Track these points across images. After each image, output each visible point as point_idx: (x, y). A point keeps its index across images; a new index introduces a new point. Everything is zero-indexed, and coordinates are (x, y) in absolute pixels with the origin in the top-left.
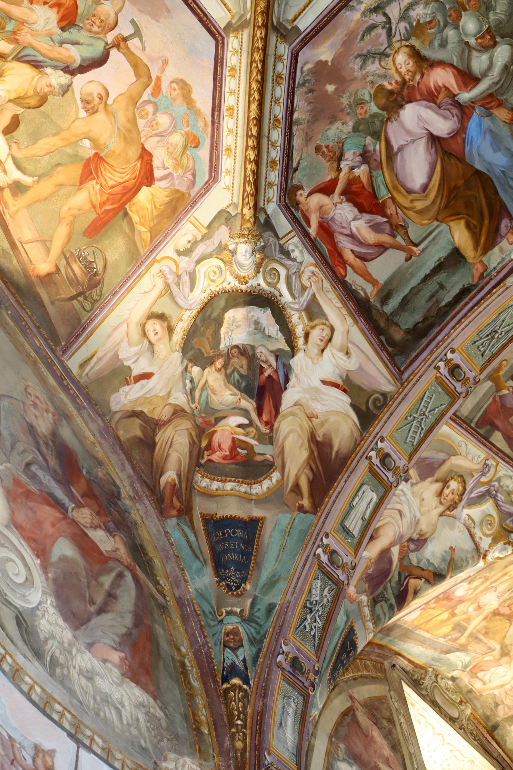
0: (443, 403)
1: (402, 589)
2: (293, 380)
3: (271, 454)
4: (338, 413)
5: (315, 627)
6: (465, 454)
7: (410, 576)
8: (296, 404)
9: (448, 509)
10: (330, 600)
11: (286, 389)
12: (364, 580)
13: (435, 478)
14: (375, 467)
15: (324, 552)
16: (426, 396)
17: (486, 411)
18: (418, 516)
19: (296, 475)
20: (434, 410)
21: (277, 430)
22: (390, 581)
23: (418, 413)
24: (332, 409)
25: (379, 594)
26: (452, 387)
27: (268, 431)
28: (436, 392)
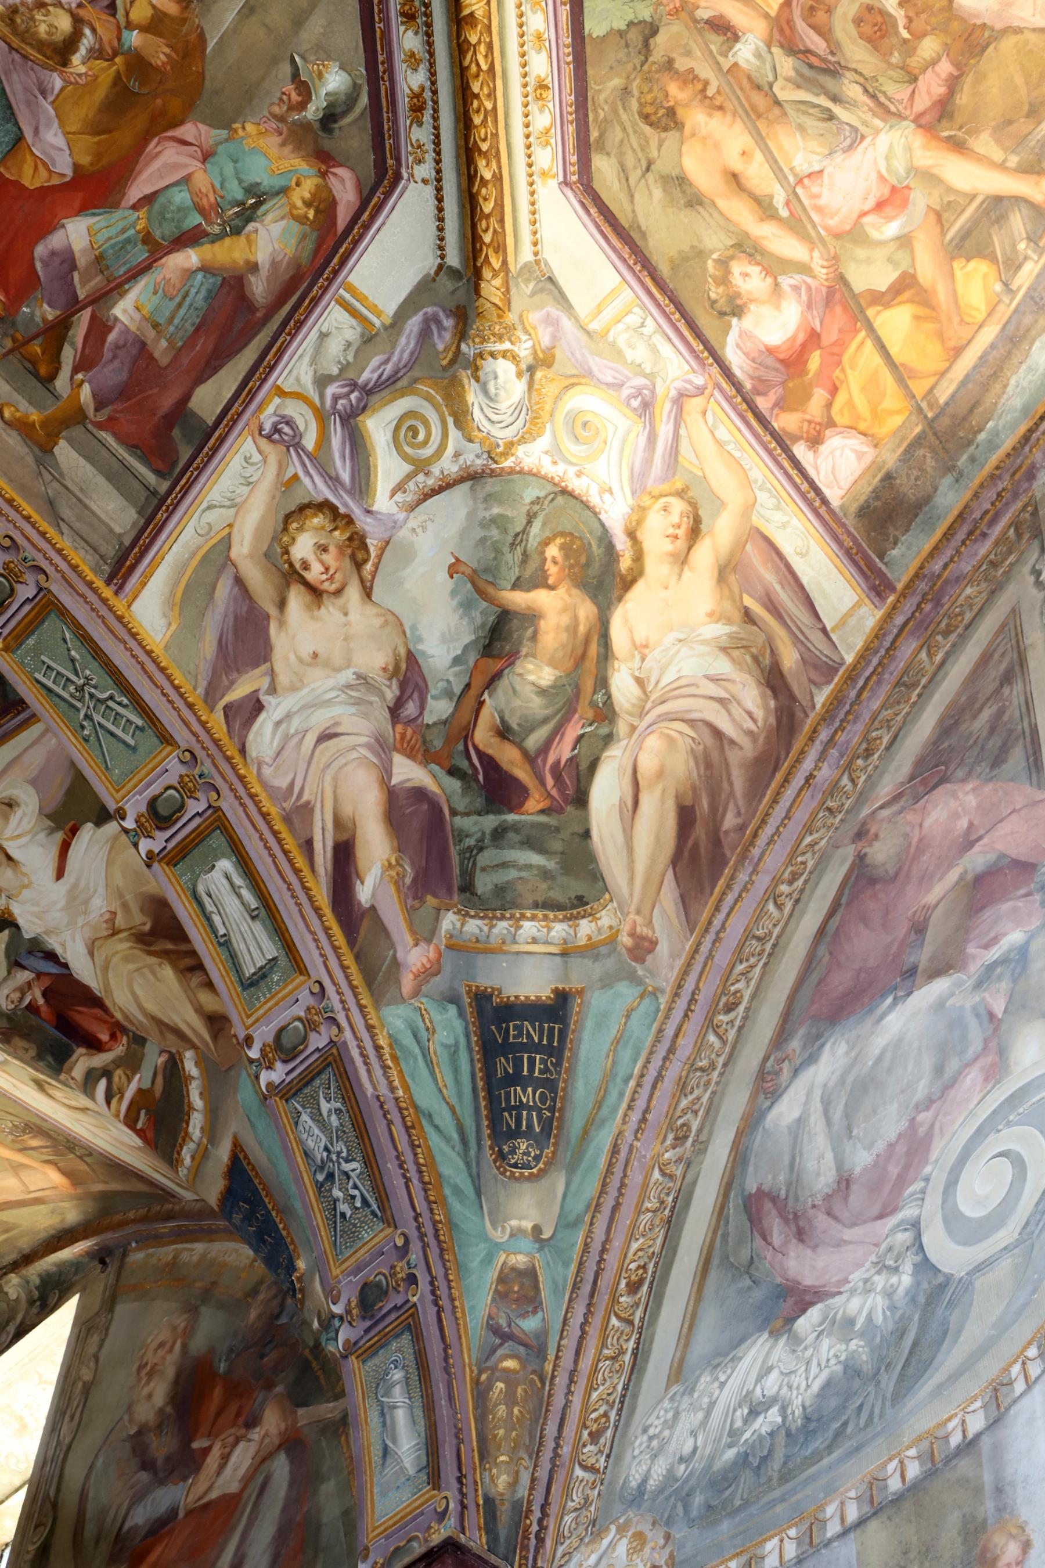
0: (59, 635)
1: (481, 778)
2: (53, 943)
3: (157, 1052)
4: (109, 862)
5: (356, 1187)
6: (233, 511)
7: (467, 734)
8: (92, 954)
9: (358, 565)
10: (339, 1105)
11: (66, 966)
12: (416, 903)
13: (273, 611)
14: (171, 845)
15: (269, 1068)
16: (44, 680)
17: (132, 447)
18: (347, 676)
19: (196, 1011)
20: (73, 660)
21: (126, 1017)
22: (454, 813)
23: (79, 705)
24: (103, 874)
25: (462, 863)
26: (27, 608)
27: (125, 1040)
28: (37, 651)
